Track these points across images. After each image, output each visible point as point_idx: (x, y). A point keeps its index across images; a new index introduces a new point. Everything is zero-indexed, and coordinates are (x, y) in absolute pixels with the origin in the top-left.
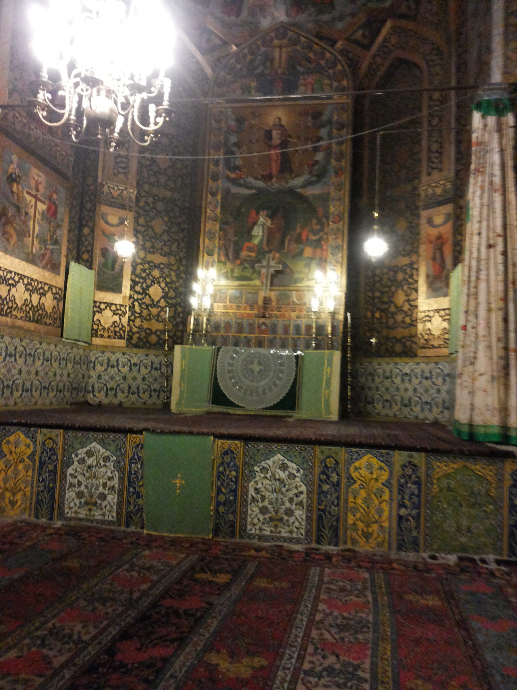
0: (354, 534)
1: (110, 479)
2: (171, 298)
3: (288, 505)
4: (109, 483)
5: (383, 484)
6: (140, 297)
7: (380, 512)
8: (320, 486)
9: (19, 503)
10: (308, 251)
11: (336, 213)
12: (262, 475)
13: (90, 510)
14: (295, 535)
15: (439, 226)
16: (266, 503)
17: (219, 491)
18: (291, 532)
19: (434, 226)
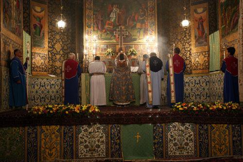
0: (215, 151)
1: (101, 137)
2: (65, 50)
3: (186, 141)
4: (101, 139)
5: (226, 128)
6: (51, 49)
7: (225, 139)
8: (199, 132)
9: (54, 154)
10: (138, 25)
11: (151, 6)
12: (174, 129)
13: (92, 153)
14: (190, 154)
15: (199, 14)
16: (176, 141)
17: (154, 138)
18: (188, 153)
19: (197, 13)
